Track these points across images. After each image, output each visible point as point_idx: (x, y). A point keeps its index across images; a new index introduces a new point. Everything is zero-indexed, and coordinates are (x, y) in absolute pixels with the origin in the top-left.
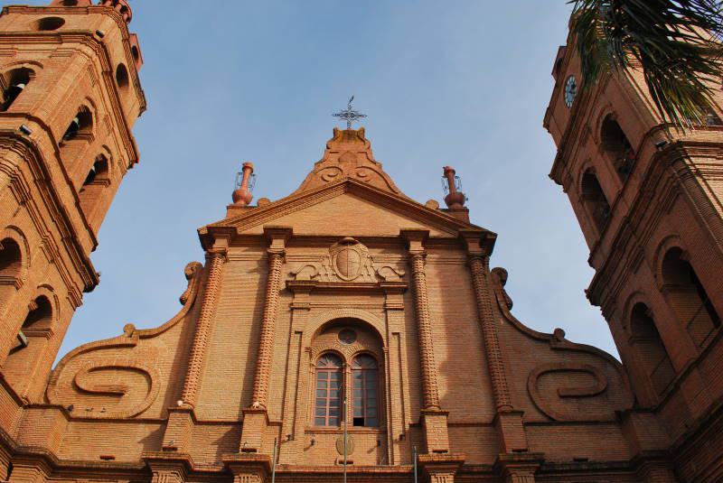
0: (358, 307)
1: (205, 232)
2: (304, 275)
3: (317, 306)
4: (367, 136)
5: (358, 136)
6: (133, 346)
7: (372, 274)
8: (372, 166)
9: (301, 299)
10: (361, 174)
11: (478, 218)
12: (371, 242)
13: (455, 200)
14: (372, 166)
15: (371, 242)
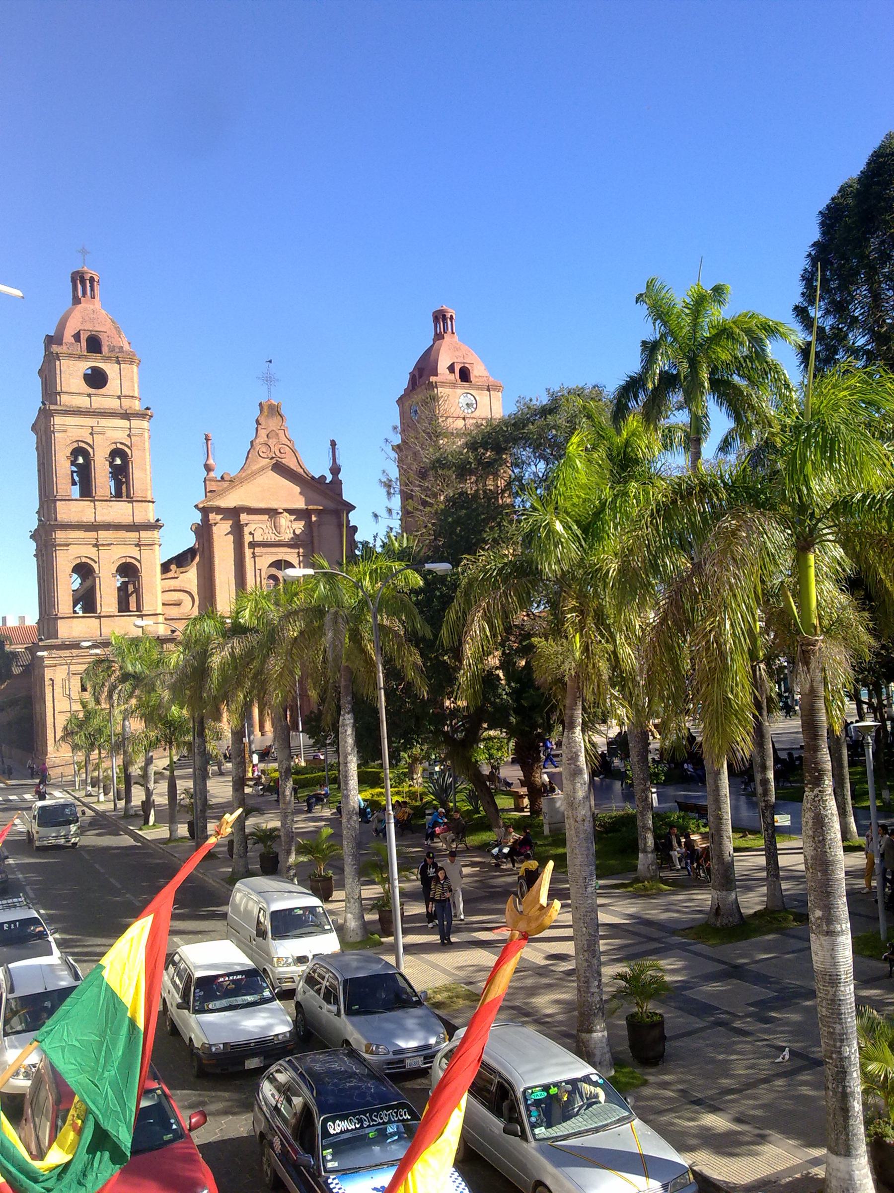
0: (286, 553)
1: (201, 506)
2: (258, 538)
3: (265, 553)
4: (282, 412)
5: (274, 411)
6: (177, 578)
7: (292, 531)
8: (288, 443)
9: (258, 550)
10: (282, 451)
11: (348, 495)
12: (290, 511)
13: (336, 470)
14: (288, 443)
15: (290, 511)
